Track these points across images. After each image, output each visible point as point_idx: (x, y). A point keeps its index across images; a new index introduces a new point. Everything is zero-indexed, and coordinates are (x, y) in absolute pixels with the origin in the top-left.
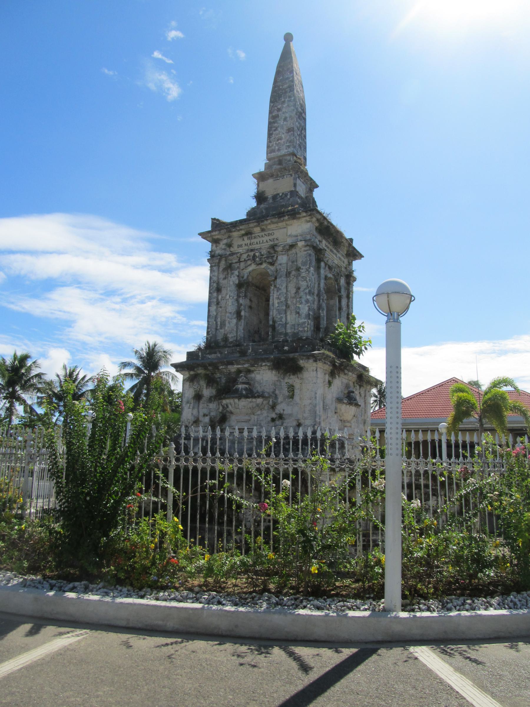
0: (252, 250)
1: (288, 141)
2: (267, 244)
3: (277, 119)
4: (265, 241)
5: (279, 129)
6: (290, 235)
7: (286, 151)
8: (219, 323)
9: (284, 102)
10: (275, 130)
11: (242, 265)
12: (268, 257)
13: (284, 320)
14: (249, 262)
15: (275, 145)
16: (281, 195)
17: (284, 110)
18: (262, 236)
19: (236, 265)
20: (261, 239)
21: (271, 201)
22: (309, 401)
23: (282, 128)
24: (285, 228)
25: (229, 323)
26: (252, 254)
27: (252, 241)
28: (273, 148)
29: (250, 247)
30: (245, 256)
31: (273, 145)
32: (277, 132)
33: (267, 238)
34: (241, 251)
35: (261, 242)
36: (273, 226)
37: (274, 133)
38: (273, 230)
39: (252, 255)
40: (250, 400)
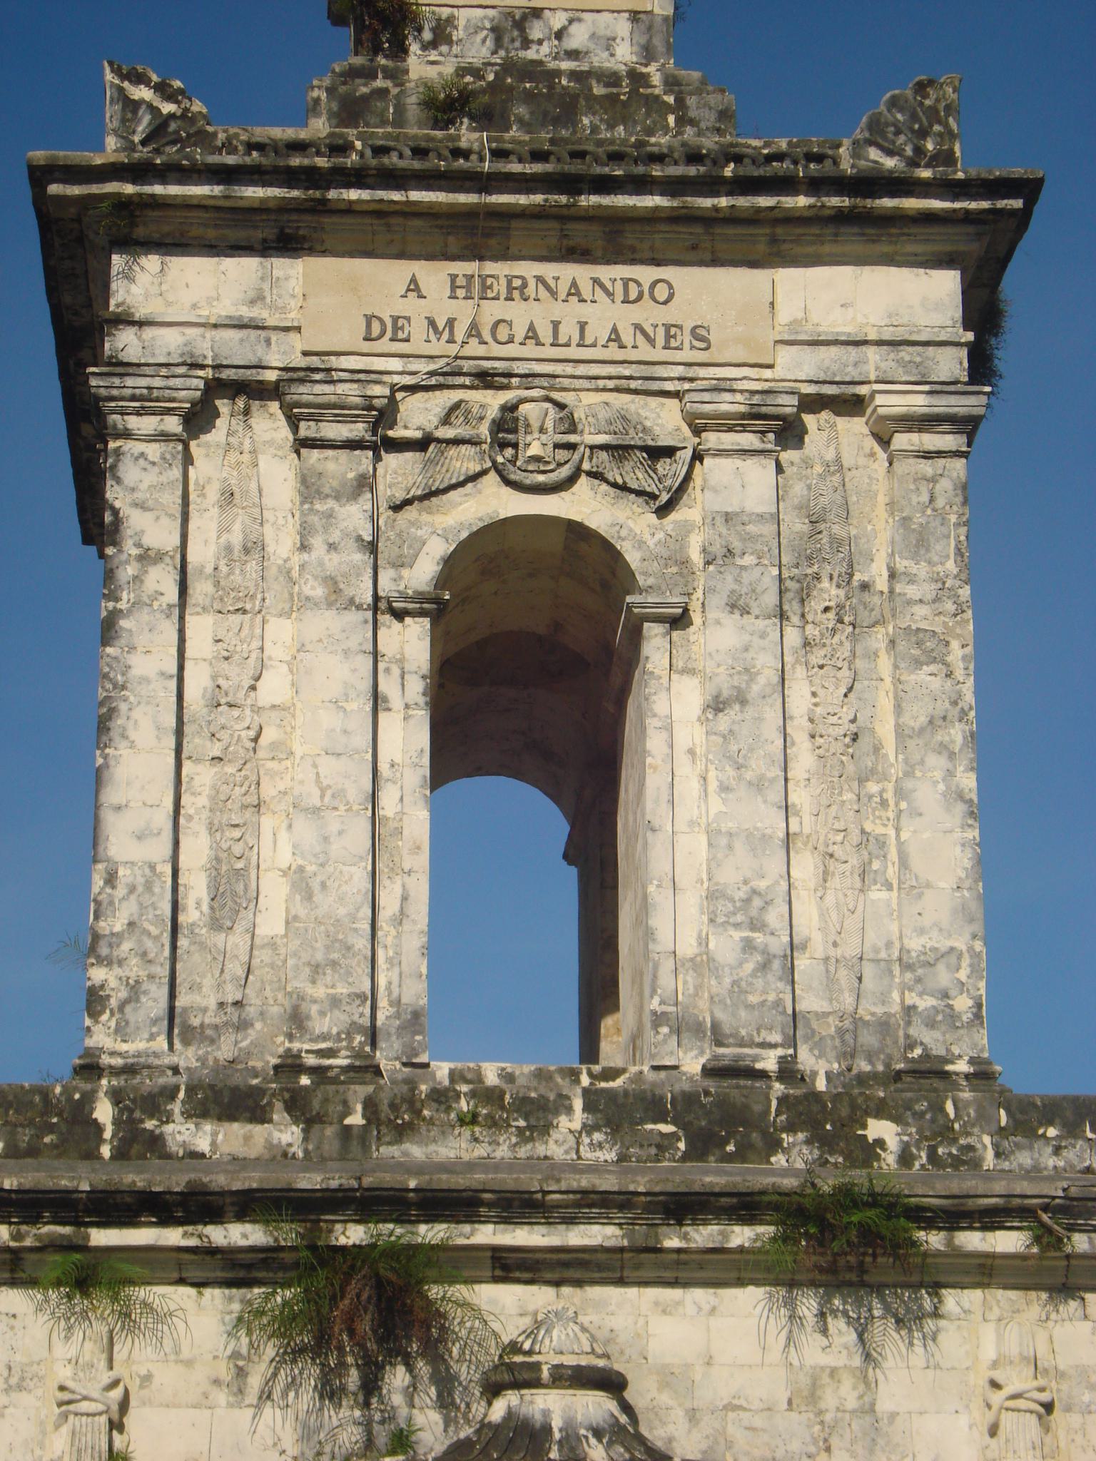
2: (613, 352)
14: (463, 461)
16: (558, 21)
18: (574, 291)
26: (493, 401)
27: (492, 311)
33: (625, 317)
35: (569, 330)
39: (493, 412)
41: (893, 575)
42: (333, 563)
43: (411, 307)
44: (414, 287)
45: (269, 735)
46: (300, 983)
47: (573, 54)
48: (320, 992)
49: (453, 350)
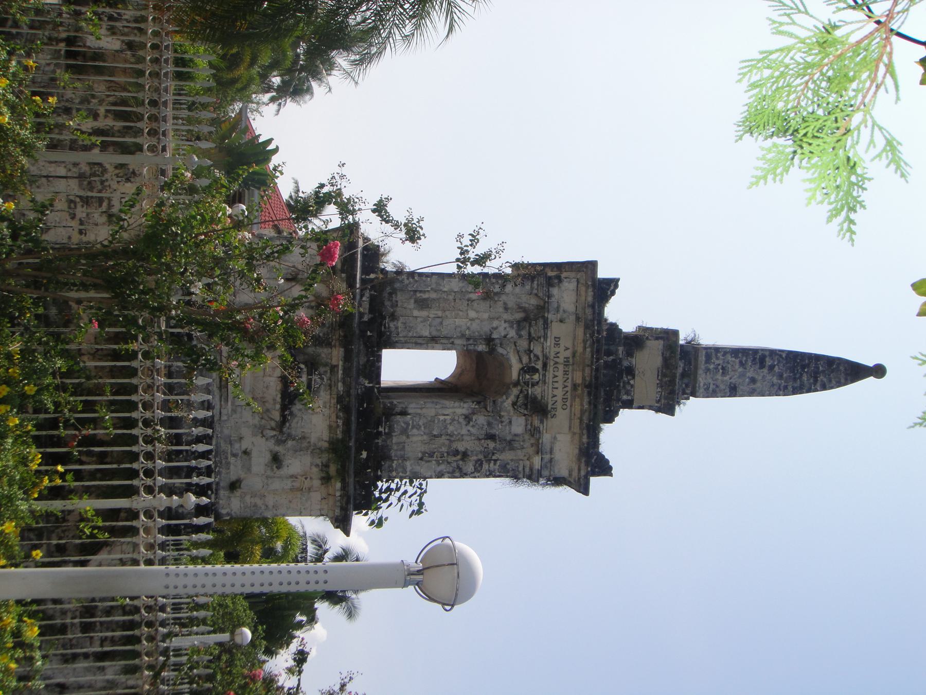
0: (545, 366)
1: (717, 386)
3: (758, 366)
4: (556, 392)
5: (741, 370)
6: (555, 438)
7: (702, 384)
8: (426, 296)
9: (780, 376)
10: (741, 362)
11: (523, 344)
12: (526, 397)
13: (415, 431)
14: (525, 359)
15: (717, 362)
16: (632, 382)
17: (769, 377)
18: (566, 387)
19: (524, 333)
20: (560, 385)
21: (625, 363)
22: (271, 504)
23: (742, 375)
24: (570, 428)
25: (425, 320)
26: (539, 366)
27: (561, 367)
28: (714, 360)
29: (552, 363)
30: (537, 350)
31: (717, 358)
32: (737, 367)
33: (559, 398)
34: (548, 344)
35: (556, 385)
36: (577, 408)
37: (737, 361)
38: (571, 406)
40: (279, 399)
41: (495, 461)
42: (501, 329)
43: (562, 349)
44: (567, 349)
45: (461, 313)
46: (402, 319)
47: (624, 387)
48: (400, 324)
49: (552, 357)
